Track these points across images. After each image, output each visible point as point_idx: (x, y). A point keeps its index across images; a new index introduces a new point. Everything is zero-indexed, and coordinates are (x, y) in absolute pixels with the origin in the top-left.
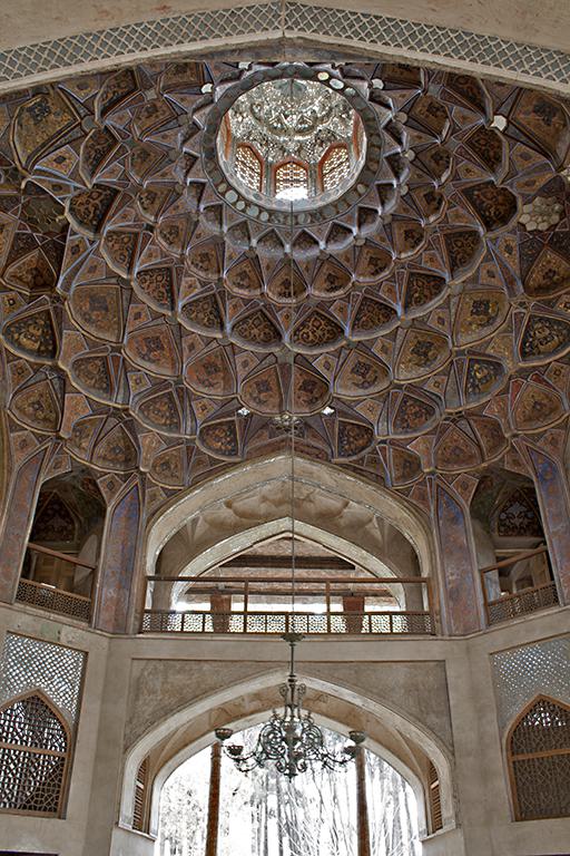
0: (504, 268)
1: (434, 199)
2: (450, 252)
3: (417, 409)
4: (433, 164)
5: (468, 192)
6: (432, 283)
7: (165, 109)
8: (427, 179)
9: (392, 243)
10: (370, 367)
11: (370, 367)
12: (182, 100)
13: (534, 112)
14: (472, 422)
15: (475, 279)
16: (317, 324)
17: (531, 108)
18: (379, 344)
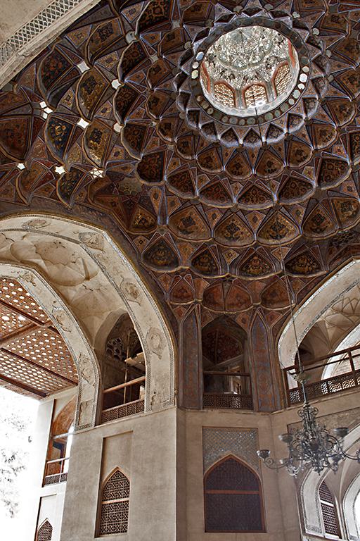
0: (117, 163)
1: (165, 128)
2: (135, 125)
3: (52, 69)
4: (184, 140)
5: (162, 154)
6: (122, 104)
7: (344, 82)
8: (180, 134)
9: (160, 90)
10: (103, 40)
11: (103, 40)
12: (336, 93)
13: (190, 217)
14: (26, 118)
15: (118, 142)
16: (157, 11)
17: (193, 216)
18: (115, 58)
